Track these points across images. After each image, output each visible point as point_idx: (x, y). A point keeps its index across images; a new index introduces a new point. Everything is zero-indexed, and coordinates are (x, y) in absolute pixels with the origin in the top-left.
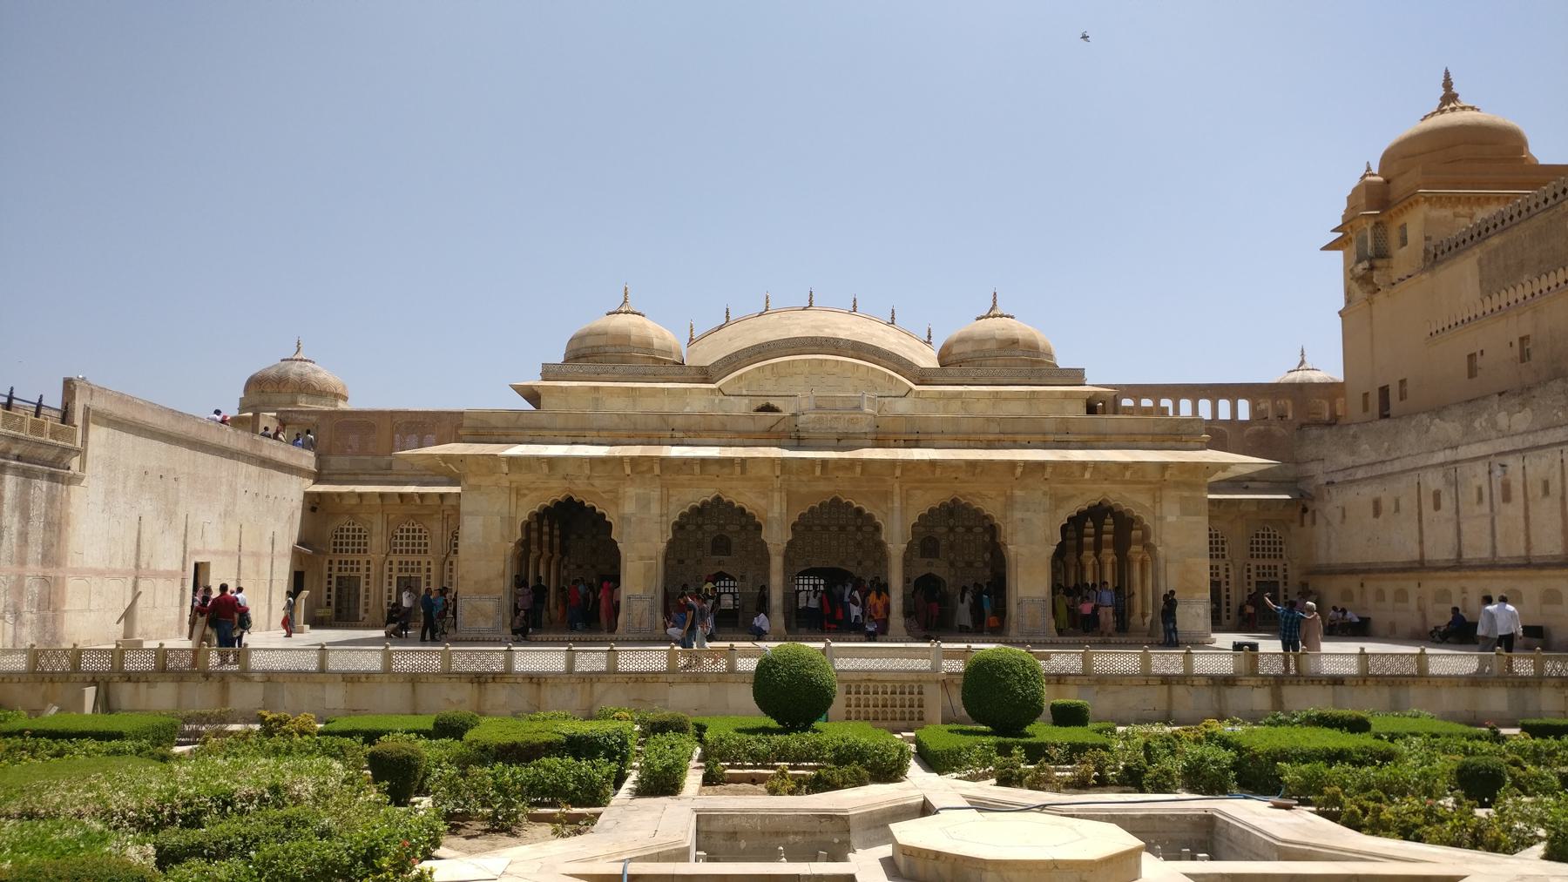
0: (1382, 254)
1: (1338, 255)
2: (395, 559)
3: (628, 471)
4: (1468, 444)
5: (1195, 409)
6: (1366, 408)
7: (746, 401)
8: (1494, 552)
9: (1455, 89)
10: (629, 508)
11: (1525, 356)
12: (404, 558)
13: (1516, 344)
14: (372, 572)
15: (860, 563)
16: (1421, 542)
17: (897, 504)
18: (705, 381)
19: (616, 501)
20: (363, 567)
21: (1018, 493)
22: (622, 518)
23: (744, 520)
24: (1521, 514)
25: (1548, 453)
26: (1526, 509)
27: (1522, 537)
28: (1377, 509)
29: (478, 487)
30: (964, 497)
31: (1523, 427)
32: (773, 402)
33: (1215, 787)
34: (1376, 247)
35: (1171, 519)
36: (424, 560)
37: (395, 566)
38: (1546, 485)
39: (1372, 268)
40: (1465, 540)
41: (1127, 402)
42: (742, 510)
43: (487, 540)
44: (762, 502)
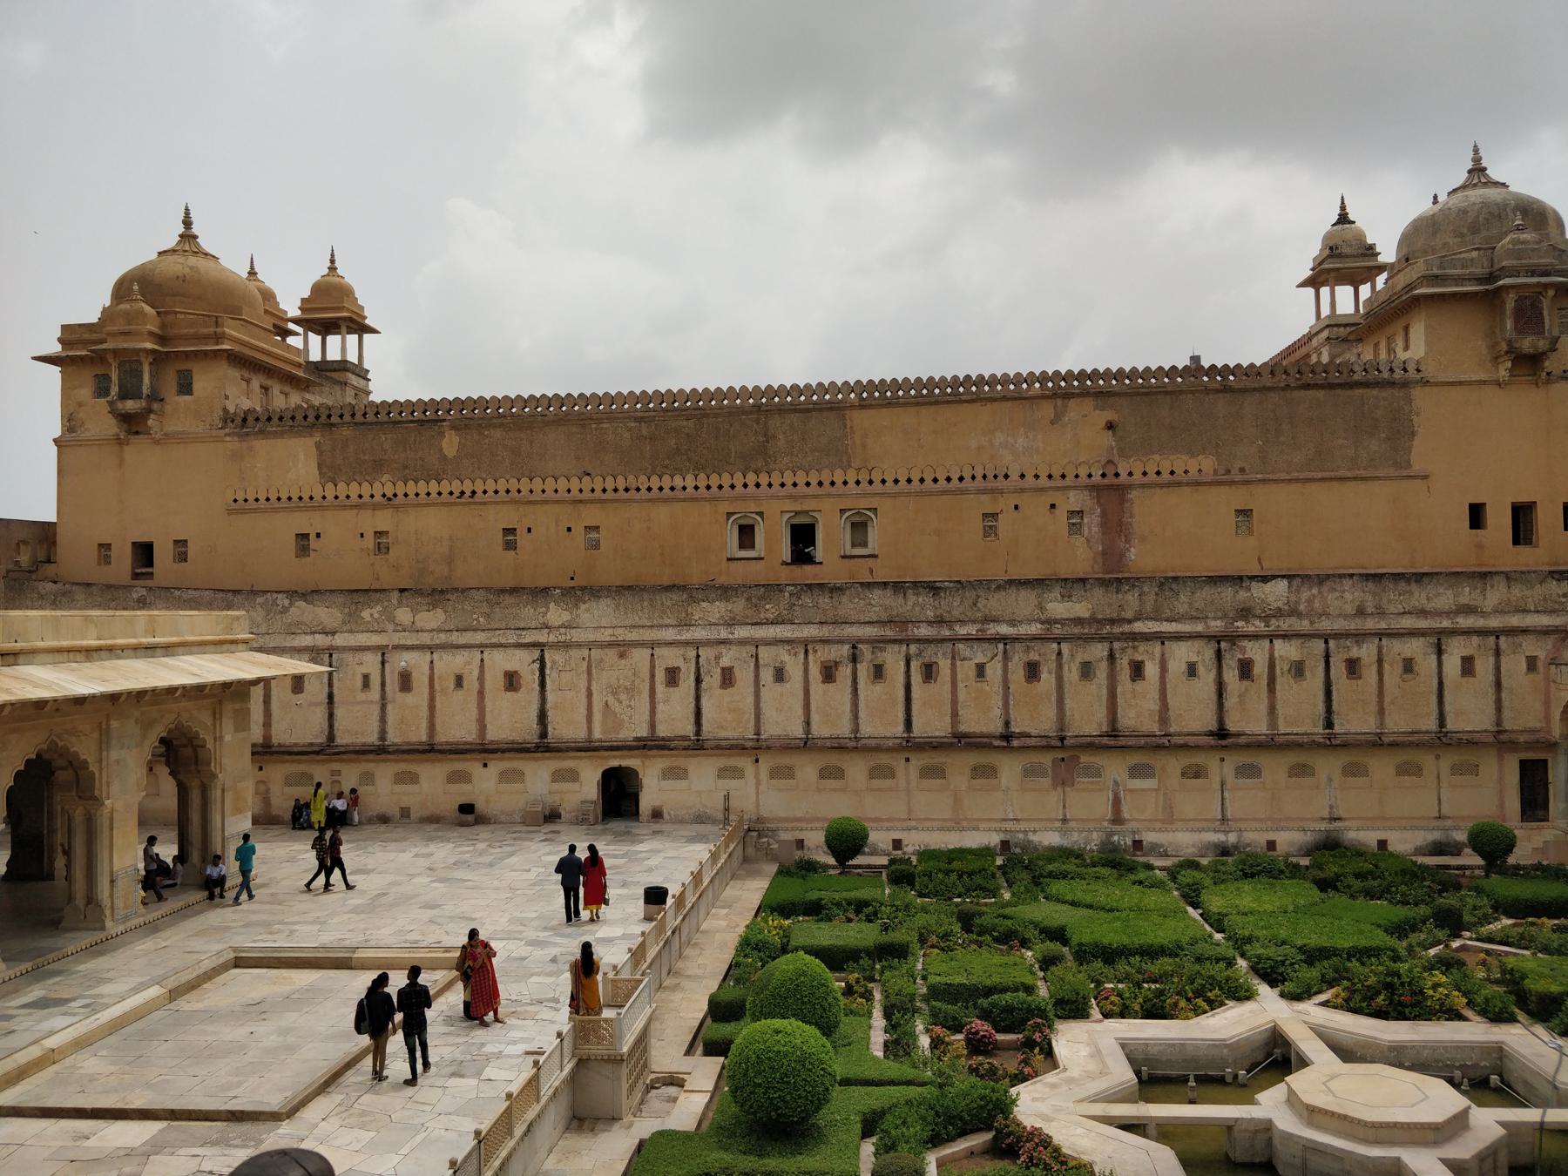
1: (55, 372)
4: (351, 631)
8: (383, 734)
9: (195, 230)
11: (382, 549)
21: (114, 724)
24: (425, 703)
25: (465, 653)
26: (432, 699)
27: (424, 725)
30: (59, 736)
31: (434, 625)
33: (1499, 1017)
34: (152, 386)
35: (228, 738)
40: (339, 725)
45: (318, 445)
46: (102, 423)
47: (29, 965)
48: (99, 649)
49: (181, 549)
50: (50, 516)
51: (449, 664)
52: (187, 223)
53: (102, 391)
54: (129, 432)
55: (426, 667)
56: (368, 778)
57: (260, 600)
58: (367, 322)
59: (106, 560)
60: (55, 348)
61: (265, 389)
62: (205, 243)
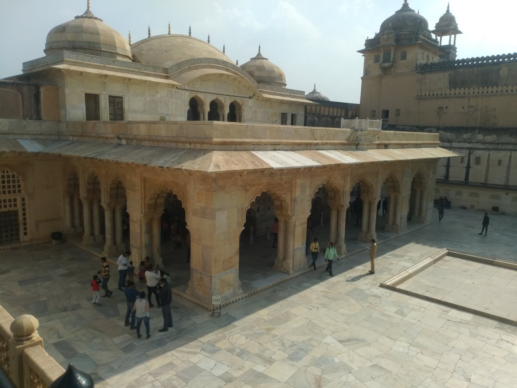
7: (187, 93)
10: (298, 193)
18: (167, 78)
35: (431, 176)
40: (450, 174)
46: (377, 71)
47: (383, 241)
49: (398, 113)
51: (495, 155)
53: (377, 60)
54: (385, 74)
55: (487, 156)
56: (459, 193)
57: (426, 130)
60: (364, 47)
61: (428, 56)
62: (411, 6)
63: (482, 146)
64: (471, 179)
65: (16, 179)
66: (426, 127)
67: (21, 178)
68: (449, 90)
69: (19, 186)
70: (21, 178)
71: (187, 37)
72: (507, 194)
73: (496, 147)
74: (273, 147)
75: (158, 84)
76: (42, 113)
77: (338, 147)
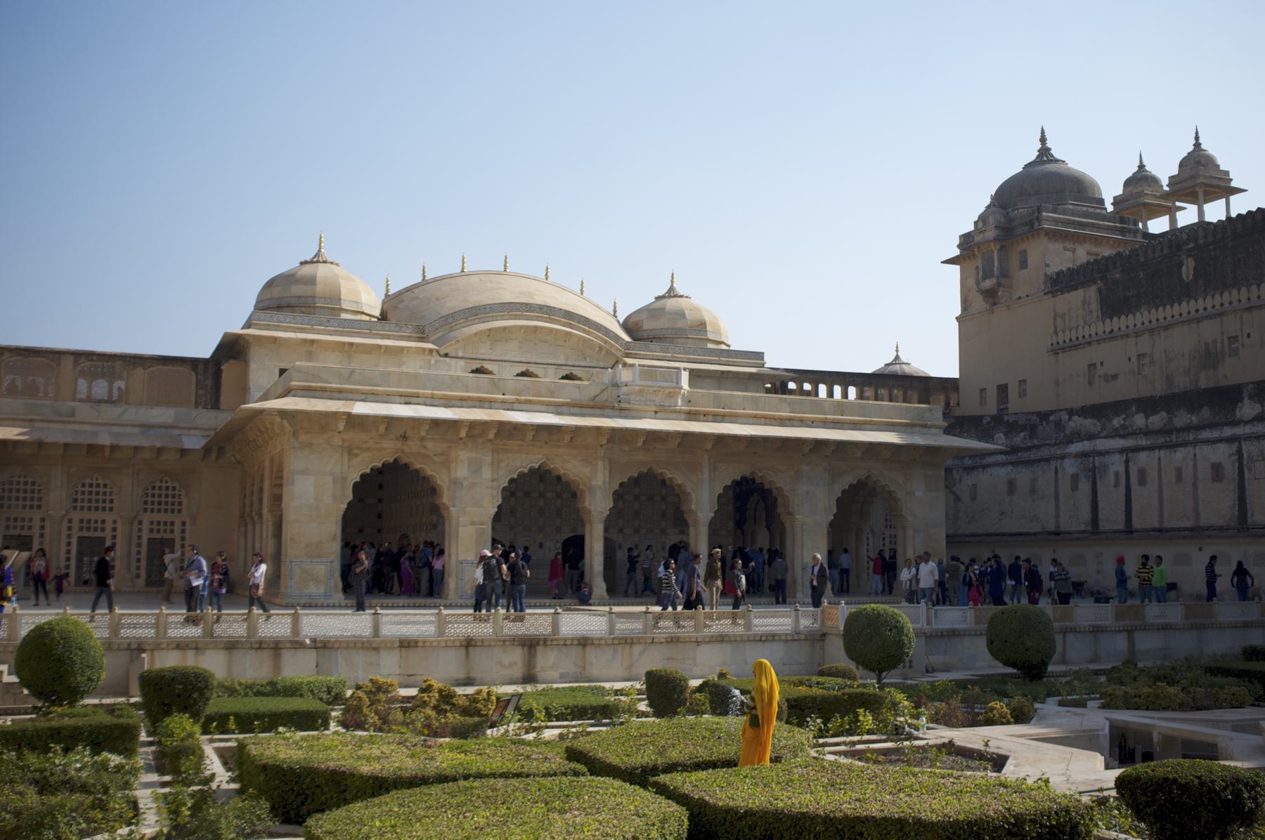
0: (1005, 274)
1: (956, 269)
2: (76, 516)
3: (463, 434)
5: (845, 395)
6: (983, 400)
7: (462, 363)
10: (461, 471)
12: (86, 515)
13: (1134, 359)
14: (47, 531)
15: (621, 531)
16: (1057, 516)
17: (706, 476)
18: (421, 339)
19: (447, 464)
20: (37, 524)
22: (455, 483)
23: (559, 488)
28: (1012, 486)
29: (310, 445)
32: (487, 366)
35: (919, 494)
36: (109, 518)
37: (76, 525)
38: (1179, 471)
39: (999, 284)
40: (1100, 516)
41: (792, 385)
42: (559, 478)
43: (315, 498)
44: (587, 470)
45: (1100, 290)
48: (790, 419)
50: (957, 376)
52: (1043, 140)
58: (1233, 184)
59: (983, 400)
60: (956, 252)
62: (1056, 153)
63: (1144, 442)
64: (1136, 524)
65: (177, 493)
66: (1052, 412)
67: (183, 493)
68: (1100, 323)
69: (180, 504)
70: (183, 493)
71: (499, 274)
72: (1200, 549)
73: (1170, 439)
74: (403, 399)
75: (403, 348)
76: (222, 399)
77: (565, 409)
